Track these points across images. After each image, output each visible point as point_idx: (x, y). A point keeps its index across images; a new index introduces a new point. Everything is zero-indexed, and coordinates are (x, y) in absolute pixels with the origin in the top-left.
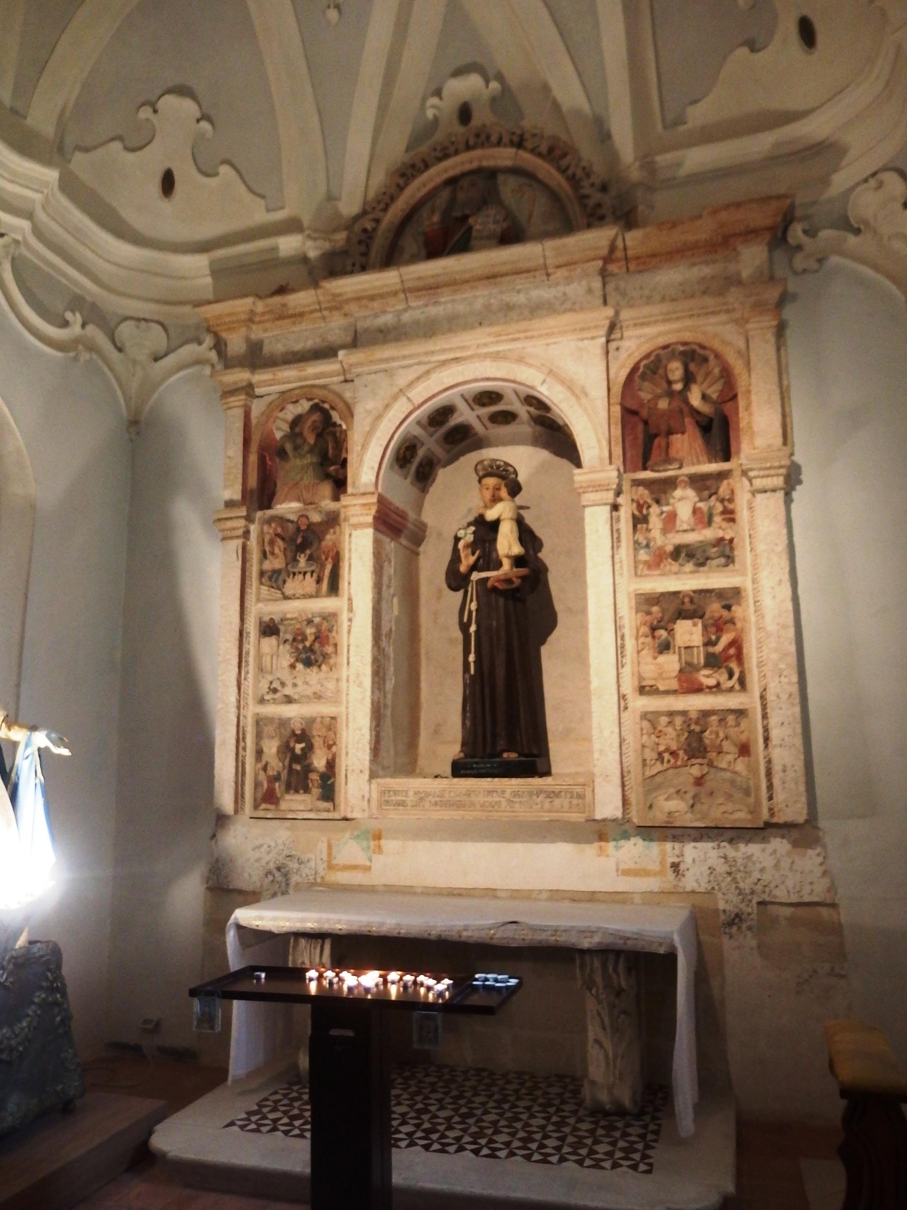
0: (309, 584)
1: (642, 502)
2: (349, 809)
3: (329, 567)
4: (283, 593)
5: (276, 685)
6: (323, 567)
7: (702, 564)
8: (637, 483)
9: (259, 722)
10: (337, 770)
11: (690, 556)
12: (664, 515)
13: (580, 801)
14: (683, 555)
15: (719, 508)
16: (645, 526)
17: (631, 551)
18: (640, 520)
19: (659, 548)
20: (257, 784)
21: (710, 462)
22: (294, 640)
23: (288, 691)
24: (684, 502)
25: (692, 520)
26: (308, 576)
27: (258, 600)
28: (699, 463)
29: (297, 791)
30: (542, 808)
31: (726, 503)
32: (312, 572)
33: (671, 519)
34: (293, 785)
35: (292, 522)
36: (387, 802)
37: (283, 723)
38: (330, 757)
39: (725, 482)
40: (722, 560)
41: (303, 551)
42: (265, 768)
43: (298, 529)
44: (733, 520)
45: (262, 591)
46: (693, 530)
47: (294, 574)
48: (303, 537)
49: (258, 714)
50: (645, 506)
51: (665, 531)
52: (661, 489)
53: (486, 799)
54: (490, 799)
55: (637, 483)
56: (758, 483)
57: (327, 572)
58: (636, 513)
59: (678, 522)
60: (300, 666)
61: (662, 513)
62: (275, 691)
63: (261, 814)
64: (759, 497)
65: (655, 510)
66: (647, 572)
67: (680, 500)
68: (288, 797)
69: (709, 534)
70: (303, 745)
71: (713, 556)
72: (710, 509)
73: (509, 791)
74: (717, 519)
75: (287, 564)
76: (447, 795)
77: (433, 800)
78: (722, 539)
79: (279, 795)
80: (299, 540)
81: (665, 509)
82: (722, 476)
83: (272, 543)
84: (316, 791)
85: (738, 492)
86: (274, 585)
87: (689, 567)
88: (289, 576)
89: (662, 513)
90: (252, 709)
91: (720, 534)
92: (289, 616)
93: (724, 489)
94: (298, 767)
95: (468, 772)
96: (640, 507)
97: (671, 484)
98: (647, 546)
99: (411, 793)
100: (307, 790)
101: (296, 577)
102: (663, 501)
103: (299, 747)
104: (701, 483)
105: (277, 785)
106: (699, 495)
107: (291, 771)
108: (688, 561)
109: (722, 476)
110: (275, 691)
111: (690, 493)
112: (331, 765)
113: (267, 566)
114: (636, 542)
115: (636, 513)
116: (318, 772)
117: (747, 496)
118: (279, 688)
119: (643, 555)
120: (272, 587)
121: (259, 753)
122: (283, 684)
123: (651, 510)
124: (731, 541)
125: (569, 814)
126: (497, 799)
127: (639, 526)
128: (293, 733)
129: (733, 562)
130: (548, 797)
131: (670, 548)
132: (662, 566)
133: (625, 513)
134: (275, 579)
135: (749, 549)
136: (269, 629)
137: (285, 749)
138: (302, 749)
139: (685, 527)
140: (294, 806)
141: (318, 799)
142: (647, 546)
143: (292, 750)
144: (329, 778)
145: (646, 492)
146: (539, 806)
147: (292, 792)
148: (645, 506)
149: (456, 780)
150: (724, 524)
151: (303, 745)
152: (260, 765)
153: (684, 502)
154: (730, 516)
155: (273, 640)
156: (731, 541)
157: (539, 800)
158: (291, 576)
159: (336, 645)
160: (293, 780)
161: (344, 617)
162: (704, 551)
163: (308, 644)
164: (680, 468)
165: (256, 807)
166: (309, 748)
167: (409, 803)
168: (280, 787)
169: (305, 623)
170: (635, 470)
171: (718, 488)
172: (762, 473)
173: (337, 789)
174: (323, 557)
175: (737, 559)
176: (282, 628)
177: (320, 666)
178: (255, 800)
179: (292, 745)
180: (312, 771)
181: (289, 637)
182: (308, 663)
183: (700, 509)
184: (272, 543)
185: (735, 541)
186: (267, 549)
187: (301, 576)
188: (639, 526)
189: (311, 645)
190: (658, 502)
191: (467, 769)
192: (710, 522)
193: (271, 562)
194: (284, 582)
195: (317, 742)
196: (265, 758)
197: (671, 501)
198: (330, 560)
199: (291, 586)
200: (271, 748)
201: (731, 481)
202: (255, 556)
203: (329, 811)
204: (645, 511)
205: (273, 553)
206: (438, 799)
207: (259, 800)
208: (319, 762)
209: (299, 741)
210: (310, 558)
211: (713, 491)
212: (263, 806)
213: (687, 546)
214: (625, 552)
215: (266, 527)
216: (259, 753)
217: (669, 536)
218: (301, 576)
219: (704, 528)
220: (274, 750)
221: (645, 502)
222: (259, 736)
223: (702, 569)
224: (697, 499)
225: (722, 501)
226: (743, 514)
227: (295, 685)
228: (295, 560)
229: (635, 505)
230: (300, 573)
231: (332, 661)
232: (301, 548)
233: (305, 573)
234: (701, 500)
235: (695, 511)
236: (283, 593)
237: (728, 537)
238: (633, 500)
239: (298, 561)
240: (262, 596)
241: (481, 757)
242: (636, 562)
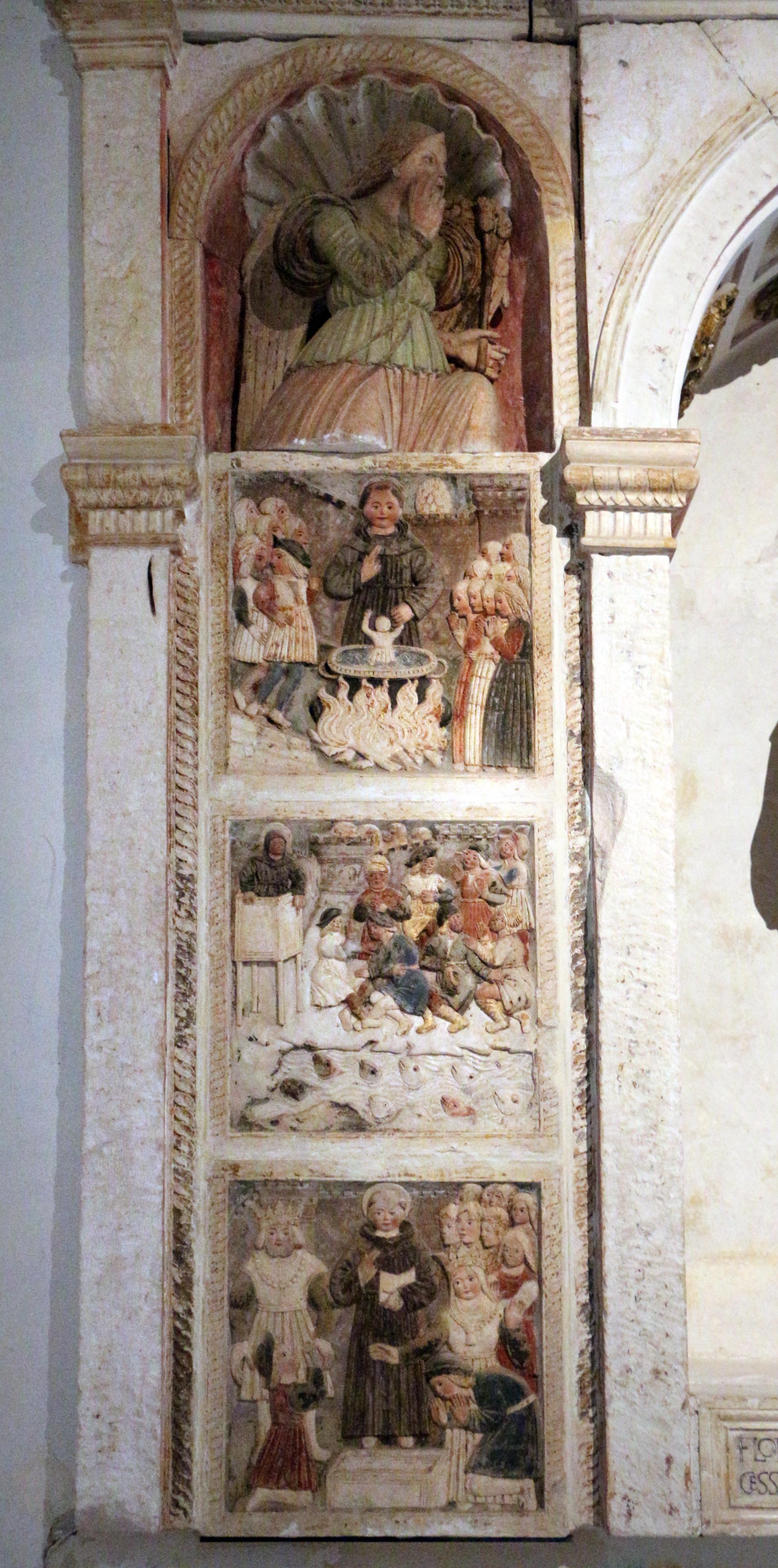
0: (413, 721)
2: (616, 1506)
3: (485, 672)
4: (316, 747)
5: (299, 1067)
6: (458, 675)
9: (245, 1191)
10: (547, 1367)
20: (239, 1414)
22: (359, 913)
23: (346, 1087)
26: (409, 692)
27: (224, 766)
29: (388, 1440)
32: (423, 683)
34: (375, 1419)
35: (340, 505)
36: (755, 1479)
37: (336, 1200)
38: (516, 1316)
41: (384, 608)
42: (264, 1360)
43: (362, 531)
45: (235, 735)
47: (355, 684)
48: (382, 557)
49: (235, 1168)
57: (480, 689)
60: (383, 1000)
62: (293, 1090)
63: (257, 1524)
68: (353, 1460)
70: (409, 1277)
75: (324, 649)
79: (318, 1453)
80: (370, 569)
83: (265, 571)
84: (461, 1443)
86: (278, 716)
88: (334, 693)
90: (214, 1147)
92: (344, 829)
94: (394, 1355)
100: (426, 1435)
101: (360, 696)
103: (391, 1287)
105: (310, 1416)
107: (358, 1364)
110: (293, 1090)
112: (518, 1349)
113: (250, 647)
116: (466, 1373)
118: (311, 1077)
120: (278, 726)
121: (242, 1302)
122: (325, 1067)
128: (368, 1233)
134: (277, 692)
136: (267, 868)
137: (344, 1293)
138: (406, 1293)
140: (381, 1495)
141: (473, 1468)
143: (364, 1298)
144: (515, 1393)
147: (370, 1442)
151: (409, 1277)
152: (247, 1348)
155: (286, 911)
158: (343, 692)
159: (527, 936)
160: (375, 1399)
161: (557, 849)
163: (413, 929)
165: (234, 1501)
166: (432, 1290)
168: (319, 1420)
169: (404, 856)
173: (548, 1429)
174: (461, 635)
176: (312, 869)
177: (462, 1008)
178: (230, 1476)
179: (366, 1273)
180: (446, 1369)
181: (345, 903)
182: (417, 1000)
184: (265, 571)
186: (250, 586)
187: (382, 695)
189: (428, 932)
193: (264, 639)
194: (316, 710)
195: (468, 1266)
196: (262, 1322)
198: (488, 648)
199: (347, 723)
200: (288, 1280)
202: (209, 614)
203: (520, 1509)
205: (269, 606)
207: (240, 1471)
208: (471, 1328)
209: (389, 1265)
210: (408, 637)
212: (262, 1494)
215: (242, 511)
216: (242, 1302)
218: (382, 695)
220: (297, 1298)
222: (241, 1243)
227: (369, 1071)
228: (353, 634)
230: (376, 682)
231: (510, 993)
232: (380, 596)
233: (396, 685)
236: (316, 747)
239: (369, 641)
240: (235, 753)
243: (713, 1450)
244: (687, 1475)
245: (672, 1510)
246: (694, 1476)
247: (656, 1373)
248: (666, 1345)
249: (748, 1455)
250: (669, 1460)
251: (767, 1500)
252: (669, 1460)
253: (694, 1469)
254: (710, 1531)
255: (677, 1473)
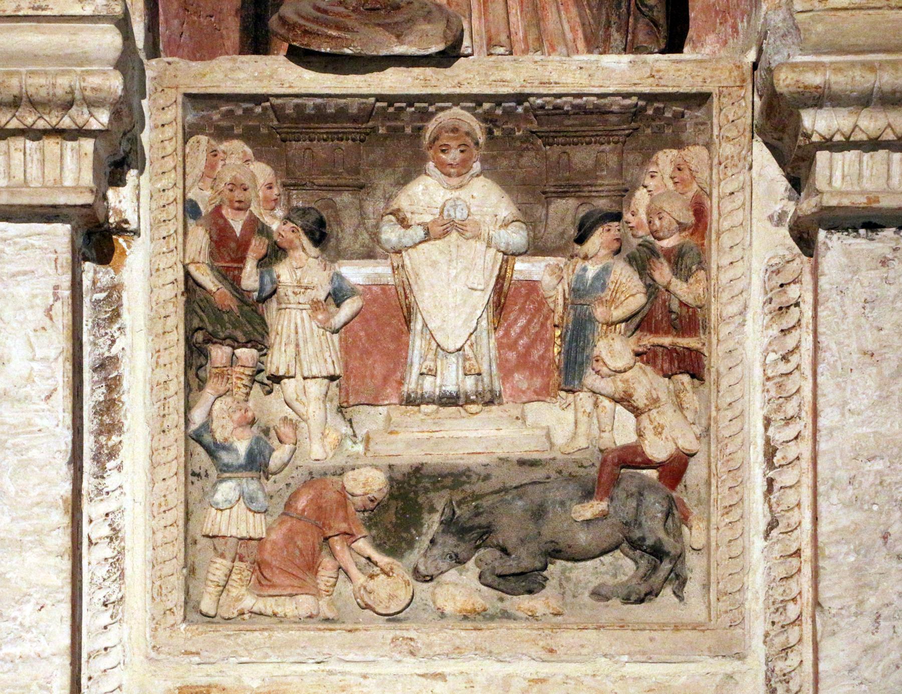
1: (237, 225)
7: (527, 581)
8: (215, 116)
11: (470, 533)
12: (349, 308)
14: (432, 524)
15: (628, 292)
16: (246, 354)
17: (174, 488)
18: (221, 323)
19: (313, 479)
21: (597, 43)
24: (454, 245)
25: (488, 346)
28: (541, 42)
31: (663, 273)
33: (384, 325)
39: (666, 159)
40: (623, 567)
44: (692, 365)
46: (491, 399)
50: (257, 247)
51: (349, 392)
52: (339, 162)
55: (215, 116)
56: (841, 178)
58: (207, 279)
59: (417, 346)
61: (337, 296)
64: (834, 247)
65: (303, 272)
66: (249, 602)
67: (428, 236)
69: (562, 427)
71: (583, 538)
72: (579, 293)
74: (614, 350)
78: (631, 458)
81: (355, 273)
82: (658, 120)
85: (723, 217)
87: (461, 588)
89: (337, 296)
91: (623, 431)
93: (656, 193)
96: (227, 249)
97: (393, 138)
98: (256, 463)
102: (346, 233)
104: (540, 146)
106: (528, 219)
108: (459, 561)
109: (658, 120)
111: (486, 201)
114: (200, 438)
115: (207, 279)
117: (771, 243)
119: (233, 511)
123: (284, 272)
124: (674, 470)
127: (219, 354)
129: (679, 580)
131: (368, 482)
132: (326, 574)
133: (146, 275)
135: (757, 511)
139: (451, 379)
142: (256, 463)
145: (263, 172)
148: (257, 247)
150: (645, 382)
153: (454, 245)
154: (677, 342)
156: (674, 470)
162: (539, 513)
164: (448, 56)
170: (204, 49)
171: (625, 193)
172: (870, 123)
175: (694, 564)
183: (532, 286)
185: (695, 472)
188: (219, 354)
190: (319, 234)
192: (571, 369)
197: (391, 234)
201: (695, 155)
204: (250, 278)
211: (603, 204)
213: (454, 478)
214: (135, 488)
217: (371, 419)
219: (543, 394)
221: (256, 227)
223: (525, 602)
224: (517, 237)
225: (642, 260)
226: (744, 342)
229: (200, 238)
234: (536, 248)
235: (504, 298)
237: (658, 450)
238: (191, 210)
242: (193, 544)
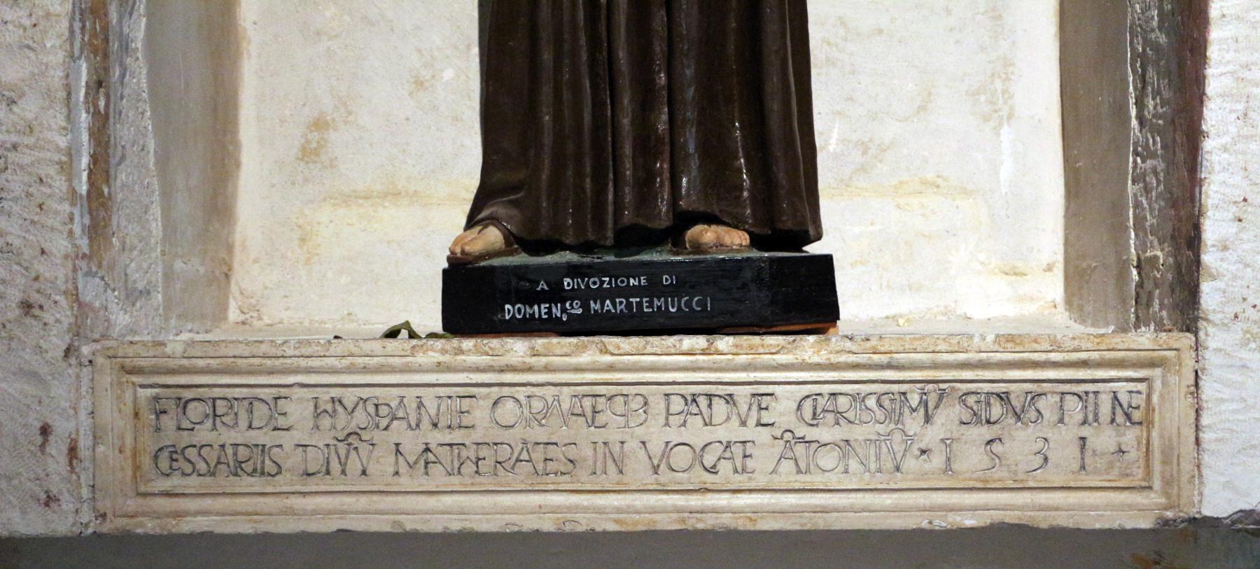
13: (1130, 437)
30: (948, 468)
36: (175, 454)
53: (674, 436)
54: (696, 433)
73: (786, 399)
76: (480, 413)
77: (412, 444)
95: (539, 310)
99: (298, 410)
125: (1073, 498)
126: (729, 431)
130: (977, 418)
146: (937, 461)
149: (472, 349)
157: (932, 435)
167: (293, 460)
191: (532, 298)
206: (435, 438)
241: (585, 248)
243: (114, 416)
244: (73, 451)
245: (50, 500)
246: (84, 452)
247: (27, 306)
248: (40, 267)
249: (168, 422)
250: (45, 431)
251: (193, 483)
252: (45, 431)
253: (84, 443)
254: (106, 528)
255: (58, 448)
